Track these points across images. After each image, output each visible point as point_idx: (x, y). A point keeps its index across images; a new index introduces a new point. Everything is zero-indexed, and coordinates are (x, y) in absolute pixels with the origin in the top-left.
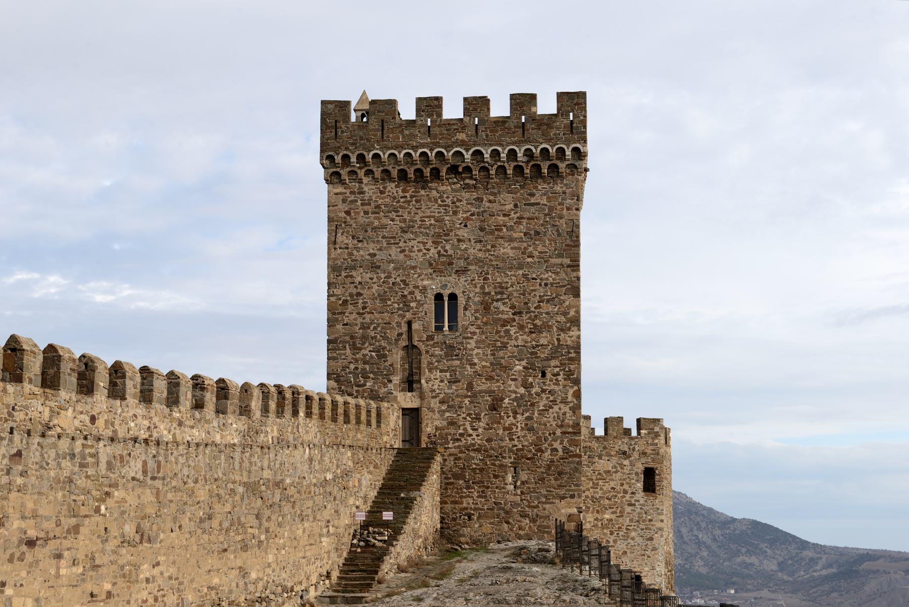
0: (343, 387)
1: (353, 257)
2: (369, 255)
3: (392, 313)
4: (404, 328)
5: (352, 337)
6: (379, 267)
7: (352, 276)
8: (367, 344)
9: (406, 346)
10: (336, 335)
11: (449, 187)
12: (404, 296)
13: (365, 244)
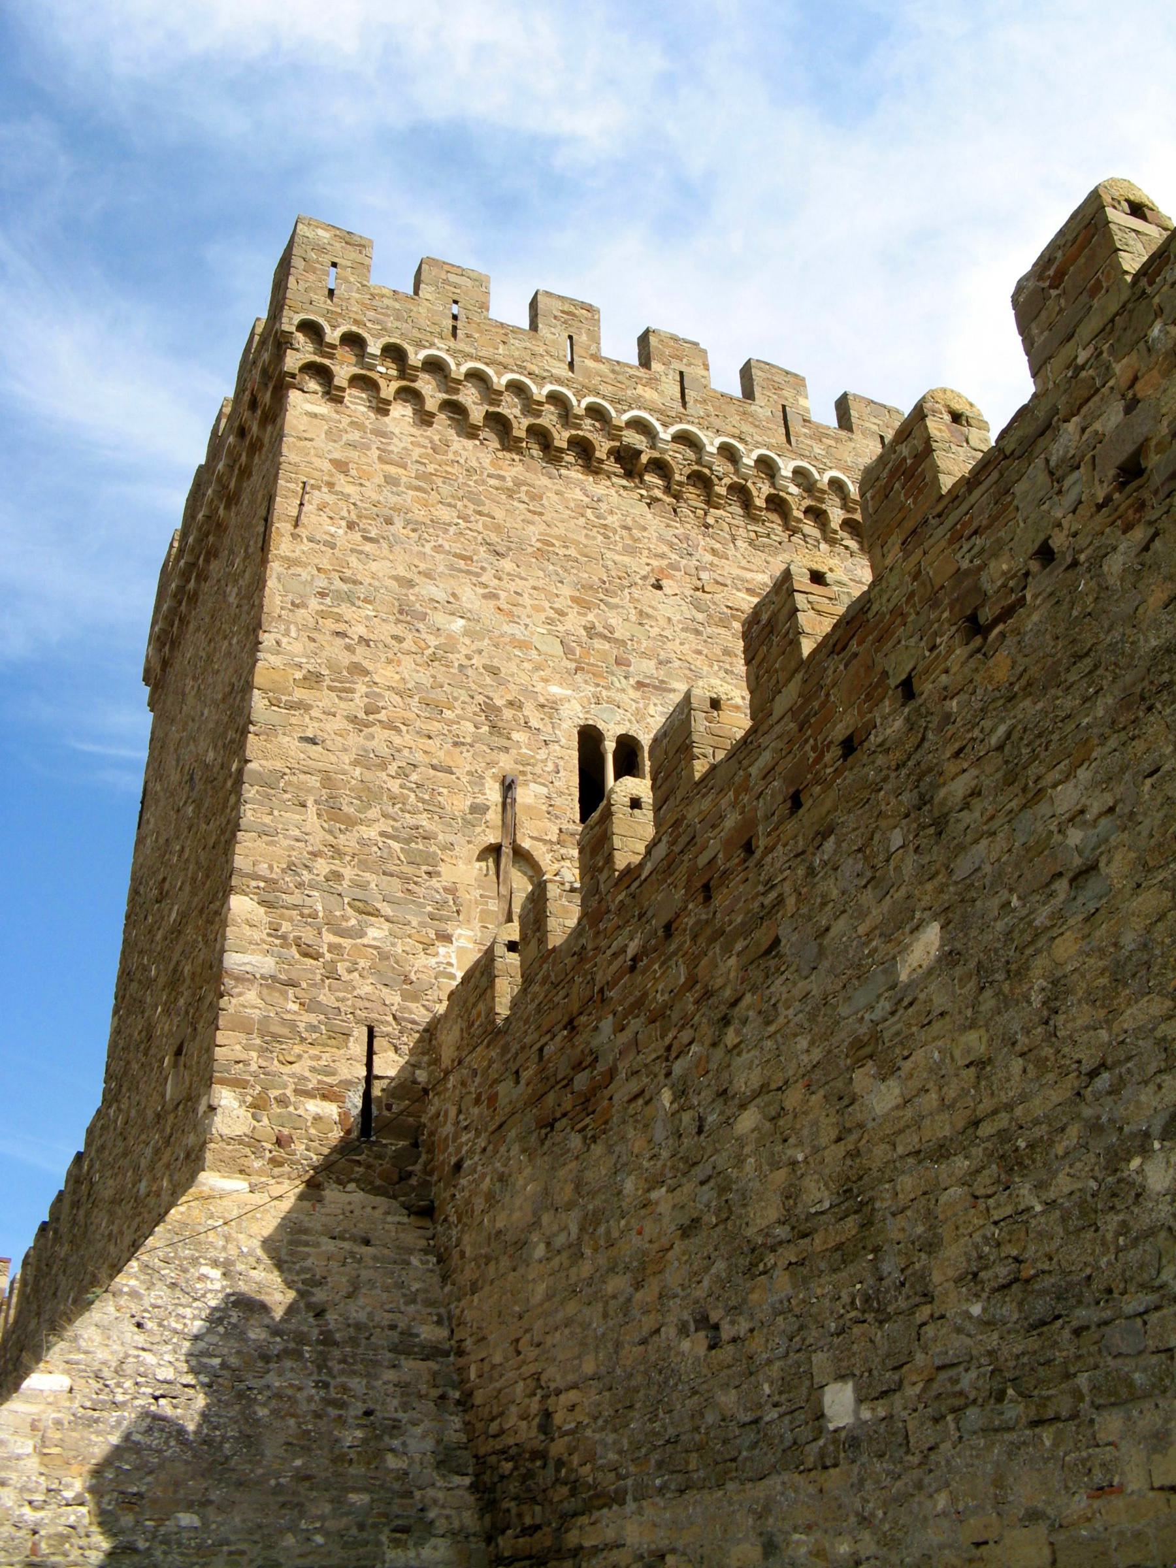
0: (286, 927)
1: (348, 573)
2: (396, 578)
3: (456, 744)
4: (493, 794)
5: (327, 780)
6: (423, 617)
7: (338, 618)
8: (373, 813)
9: (494, 851)
10: (279, 765)
11: (613, 491)
12: (489, 710)
13: (386, 552)
